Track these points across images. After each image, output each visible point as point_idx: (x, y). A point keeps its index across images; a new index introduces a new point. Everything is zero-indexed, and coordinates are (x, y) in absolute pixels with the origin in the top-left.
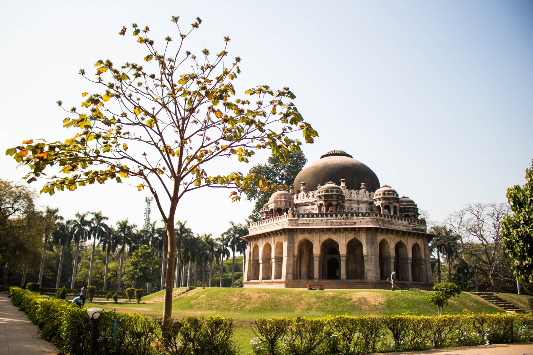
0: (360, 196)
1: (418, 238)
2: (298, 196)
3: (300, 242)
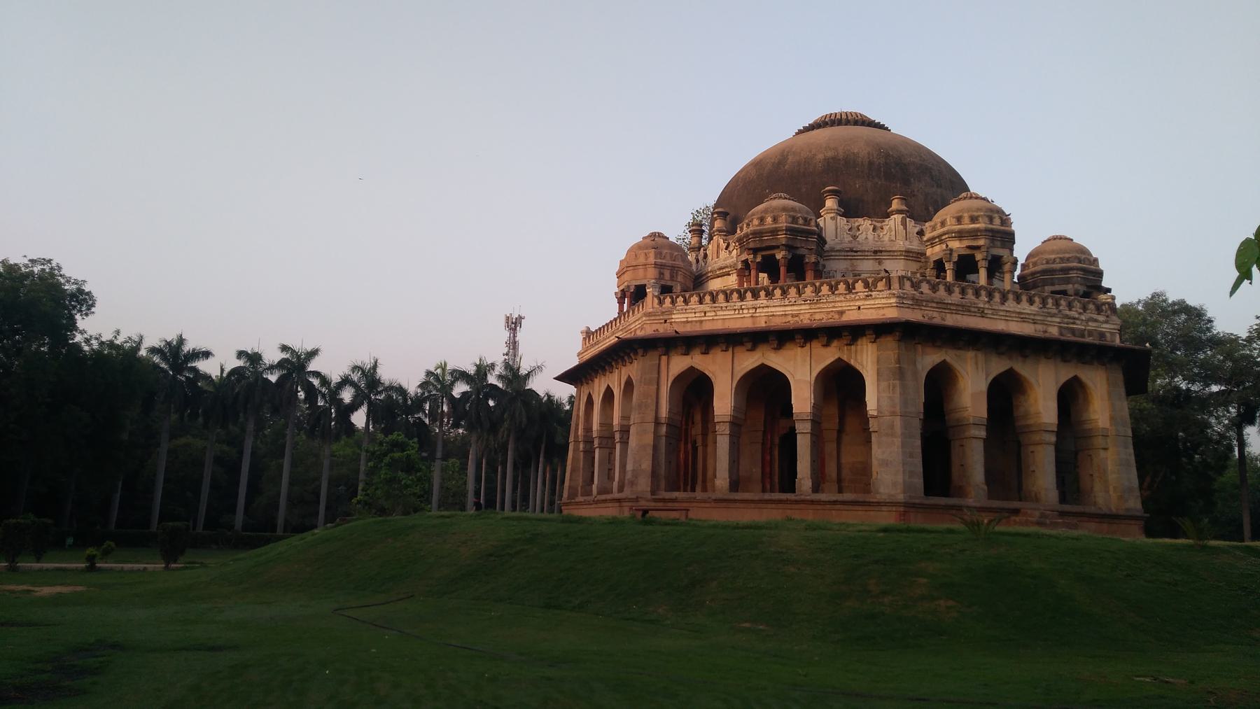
3: (673, 378)
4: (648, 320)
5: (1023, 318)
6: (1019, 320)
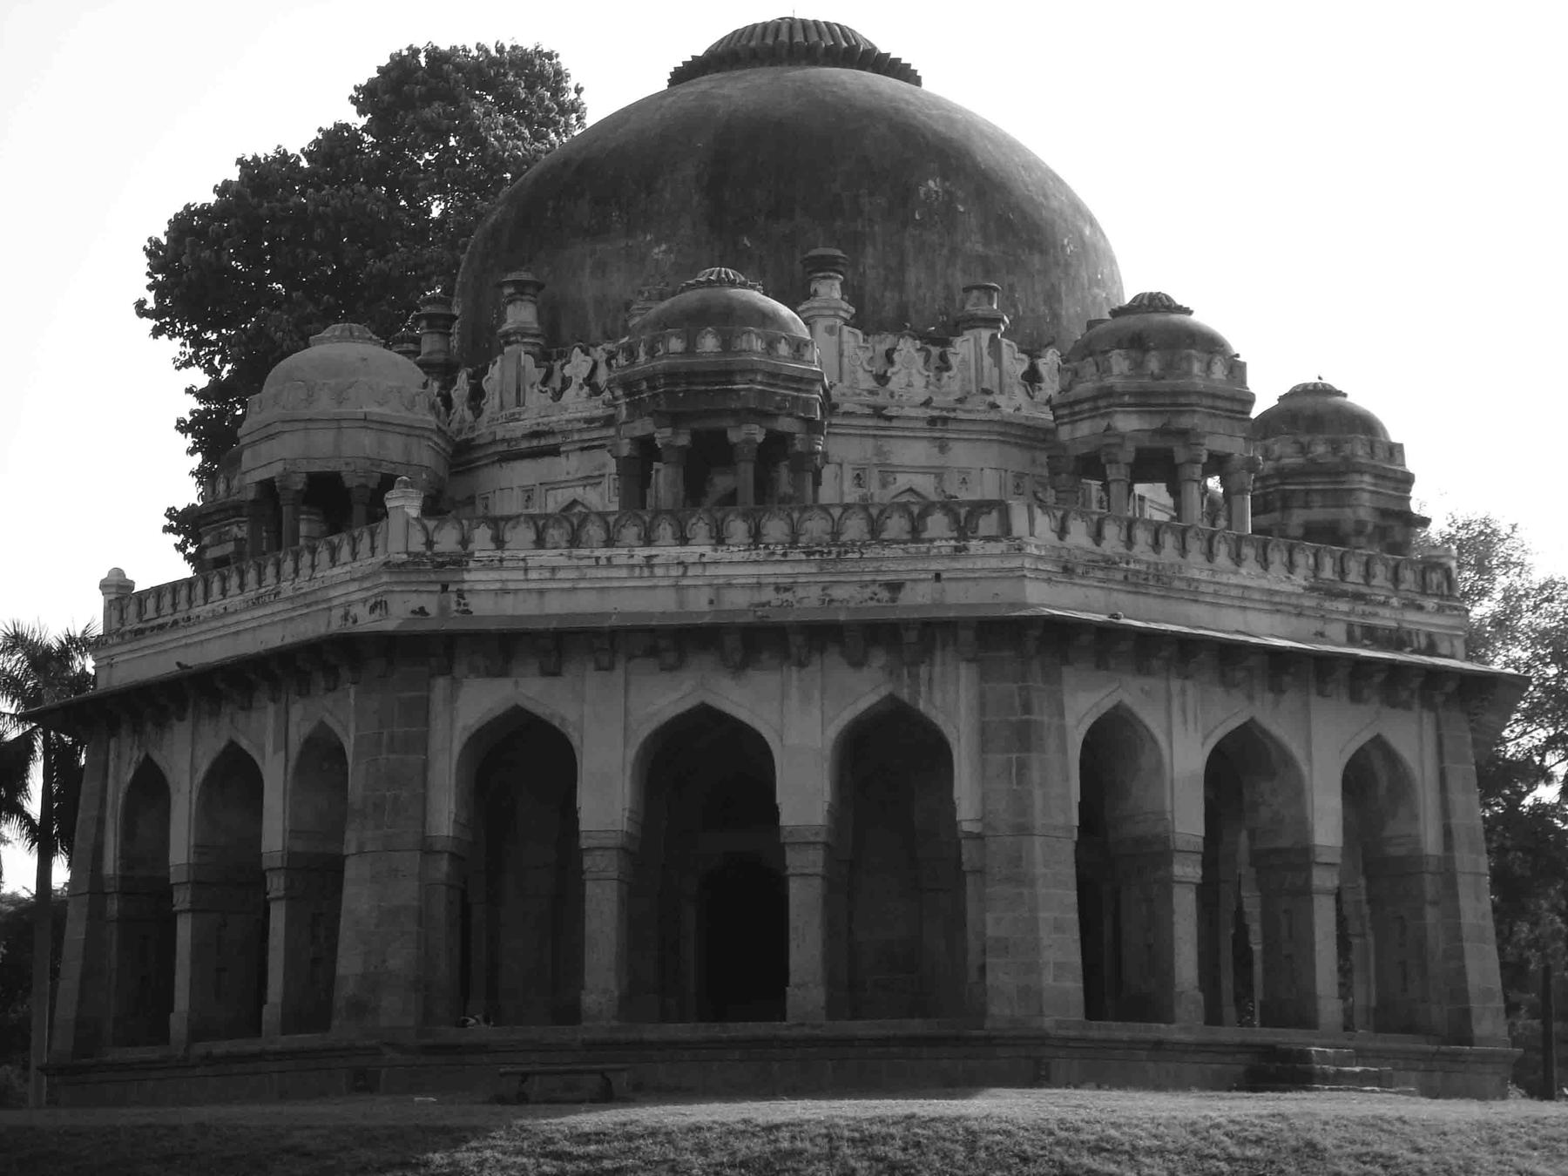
0: (953, 384)
1: (1391, 701)
2: (486, 385)
3: (466, 735)
4: (396, 583)
5: (1275, 604)
6: (1267, 607)
